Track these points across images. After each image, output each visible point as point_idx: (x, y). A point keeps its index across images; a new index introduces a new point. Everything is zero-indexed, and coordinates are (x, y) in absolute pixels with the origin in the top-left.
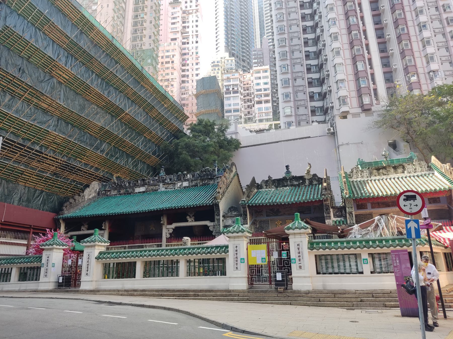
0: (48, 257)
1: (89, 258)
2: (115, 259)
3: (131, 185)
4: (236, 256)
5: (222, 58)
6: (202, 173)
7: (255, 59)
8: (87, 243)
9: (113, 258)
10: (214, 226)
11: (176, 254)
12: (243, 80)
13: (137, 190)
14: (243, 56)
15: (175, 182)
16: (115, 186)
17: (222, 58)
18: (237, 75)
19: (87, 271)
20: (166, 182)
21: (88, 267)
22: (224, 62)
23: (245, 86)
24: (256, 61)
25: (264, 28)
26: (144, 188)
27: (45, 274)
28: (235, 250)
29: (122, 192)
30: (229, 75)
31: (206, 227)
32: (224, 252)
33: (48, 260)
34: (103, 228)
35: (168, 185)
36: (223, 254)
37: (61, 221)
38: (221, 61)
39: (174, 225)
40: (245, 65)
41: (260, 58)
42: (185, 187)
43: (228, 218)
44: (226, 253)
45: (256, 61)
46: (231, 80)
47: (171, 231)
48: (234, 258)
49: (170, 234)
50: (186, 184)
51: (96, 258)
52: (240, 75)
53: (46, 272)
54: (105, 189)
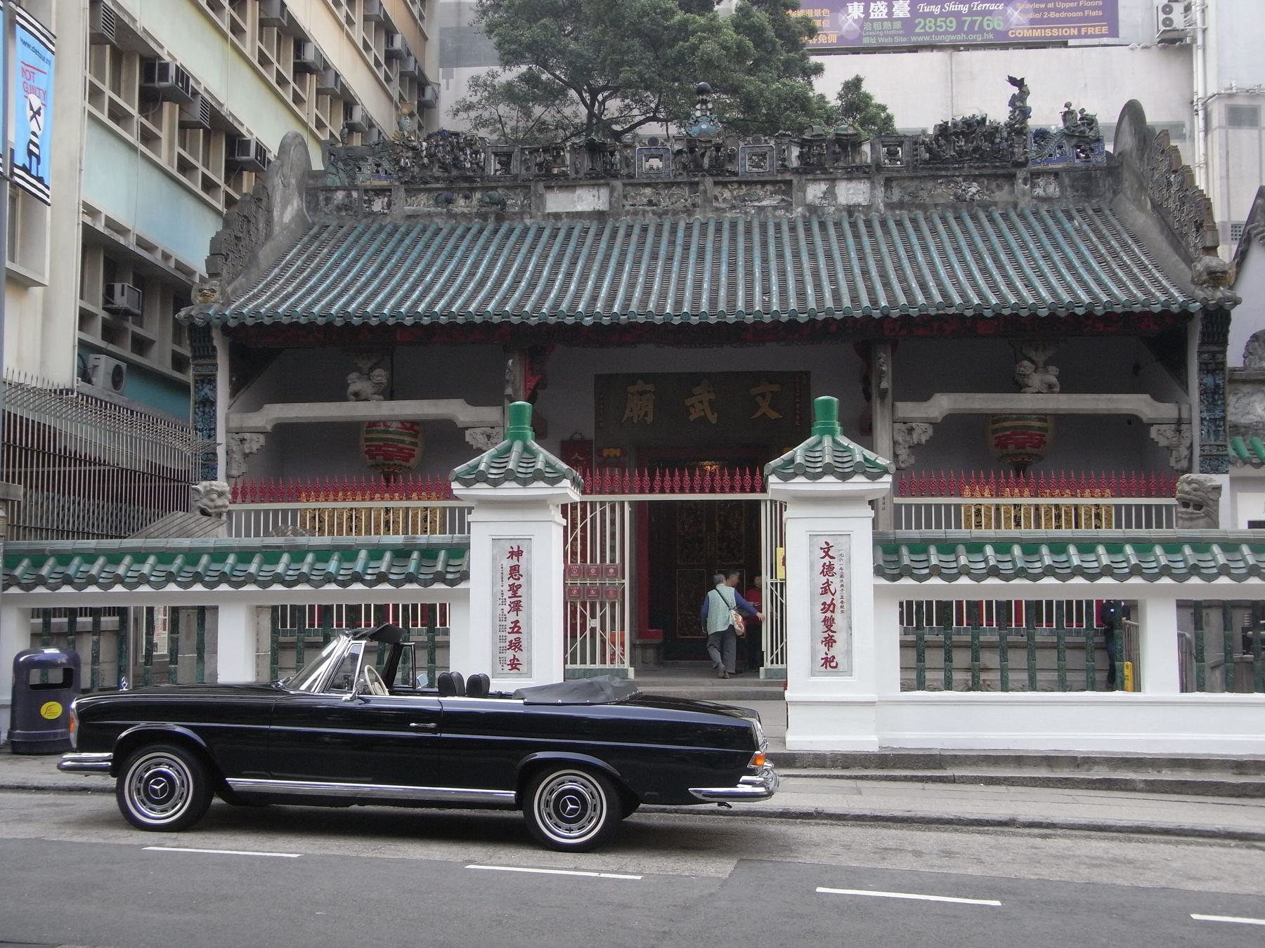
0: (517, 553)
1: (831, 567)
3: (515, 167)
6: (948, 141)
8: (819, 476)
10: (1179, 422)
13: (557, 202)
15: (788, 177)
16: (416, 169)
19: (829, 642)
20: (735, 174)
21: (828, 623)
26: (604, 192)
27: (509, 655)
29: (461, 205)
31: (1132, 422)
33: (514, 570)
34: (509, 391)
35: (744, 190)
37: (218, 341)
39: (942, 404)
42: (850, 210)
43: (1247, 389)
47: (922, 434)
49: (915, 448)
50: (852, 193)
51: (879, 571)
53: (516, 645)
54: (353, 178)
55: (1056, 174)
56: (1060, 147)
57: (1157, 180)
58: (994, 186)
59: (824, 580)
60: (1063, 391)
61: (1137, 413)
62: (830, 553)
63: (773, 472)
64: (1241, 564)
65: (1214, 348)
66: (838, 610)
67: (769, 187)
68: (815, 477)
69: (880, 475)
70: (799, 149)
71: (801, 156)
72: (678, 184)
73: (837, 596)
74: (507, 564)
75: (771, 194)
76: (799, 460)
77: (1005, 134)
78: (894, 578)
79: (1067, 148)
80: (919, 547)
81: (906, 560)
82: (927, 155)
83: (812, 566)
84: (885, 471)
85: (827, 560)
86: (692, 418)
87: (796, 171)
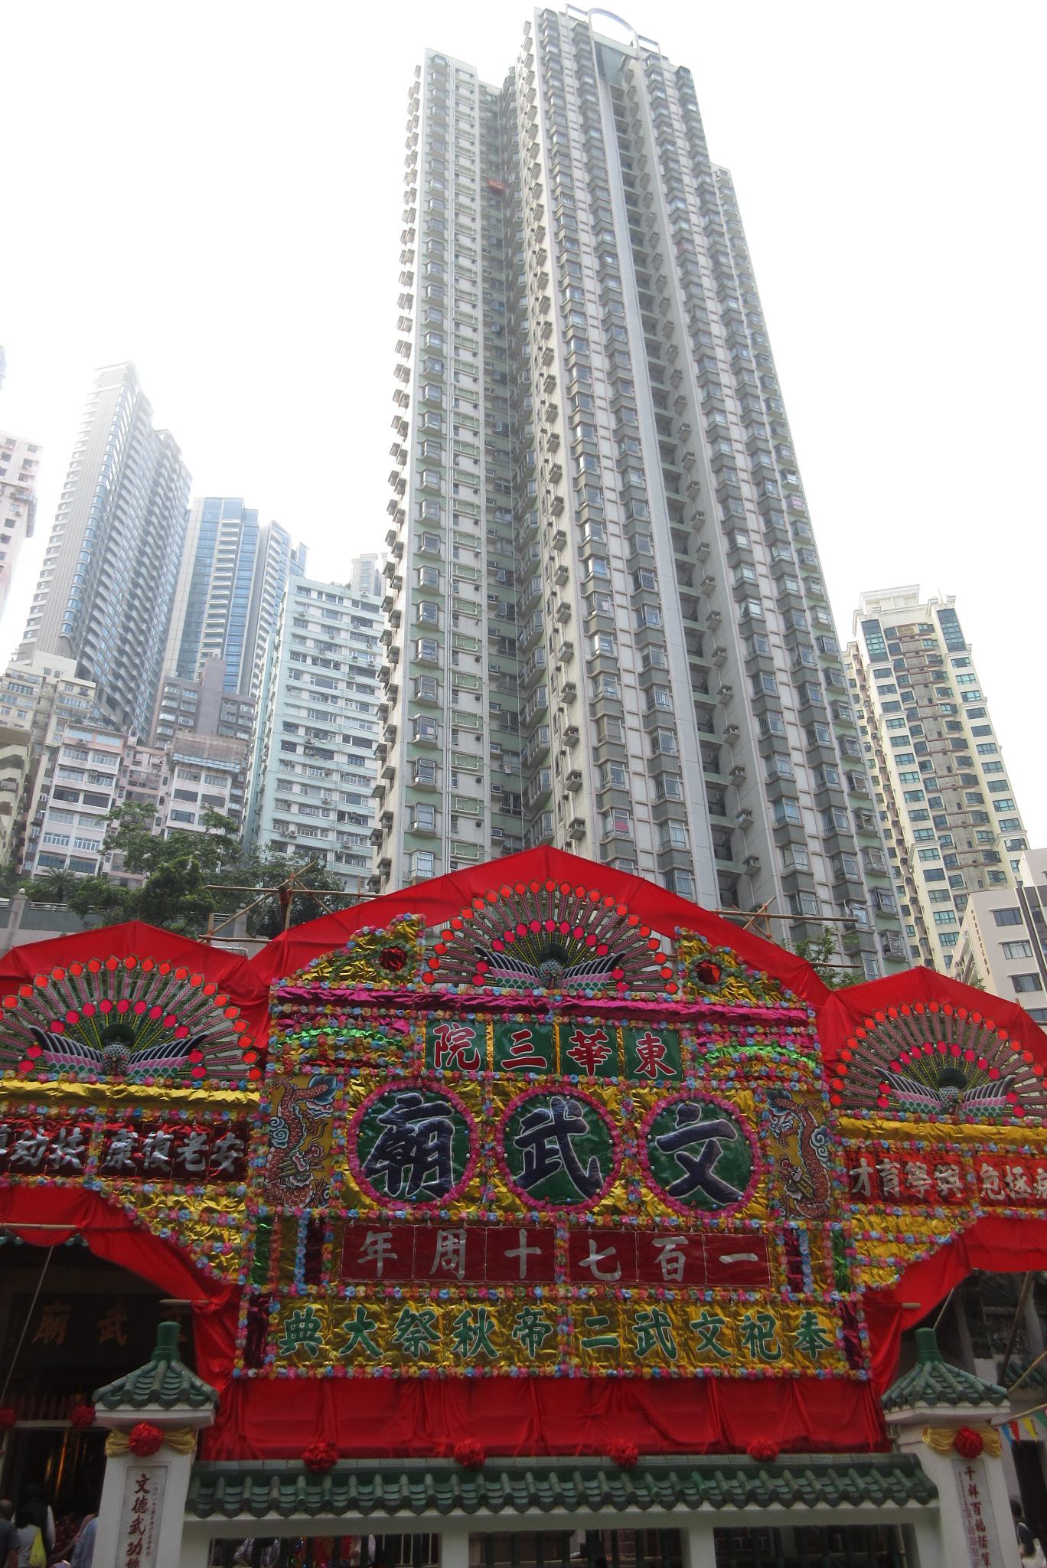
2: (322, 1516)
4: (975, 1518)
5: (47, 671)
7: (168, 710)
9: (307, 1511)
11: (681, 1497)
12: (132, 768)
14: (115, 688)
17: (47, 671)
18: (114, 744)
22: (55, 687)
23: (137, 789)
24: (170, 718)
25: (199, 624)
28: (967, 1488)
30: (86, 737)
32: (912, 1494)
36: (913, 1504)
38: (44, 679)
40: (113, 718)
41: (186, 714)
44: (923, 1501)
45: (170, 718)
46: (91, 755)
48: (970, 1531)
51: (190, 1506)
52: (125, 746)
59: (135, 1516)
62: (146, 1487)
63: (101, 1399)
64: (524, 1494)
66: (144, 1551)
68: (139, 1405)
69: (202, 1403)
73: (145, 1537)
76: (128, 1387)
78: (204, 1514)
80: (236, 1479)
81: (220, 1494)
83: (125, 1502)
84: (207, 1399)
85: (141, 1495)
86: (102, 1340)
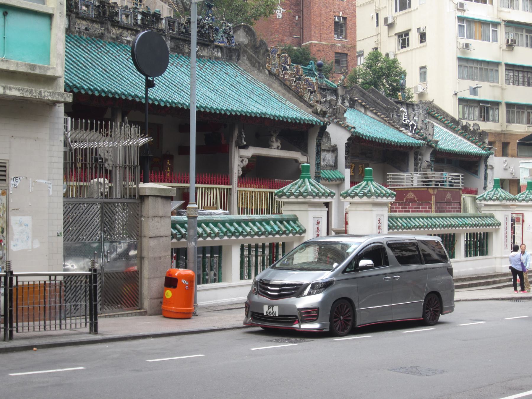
20: (118, 22)
33: (318, 228)
35: (121, 31)
47: (246, 162)
55: (221, 48)
56: (222, 37)
57: (274, 65)
58: (202, 48)
60: (282, 149)
61: (298, 159)
65: (320, 138)
67: (129, 32)
70: (141, 16)
71: (142, 20)
72: (96, 22)
74: (316, 226)
75: (130, 35)
77: (207, 27)
79: (224, 38)
82: (184, 30)
87: (140, 26)
